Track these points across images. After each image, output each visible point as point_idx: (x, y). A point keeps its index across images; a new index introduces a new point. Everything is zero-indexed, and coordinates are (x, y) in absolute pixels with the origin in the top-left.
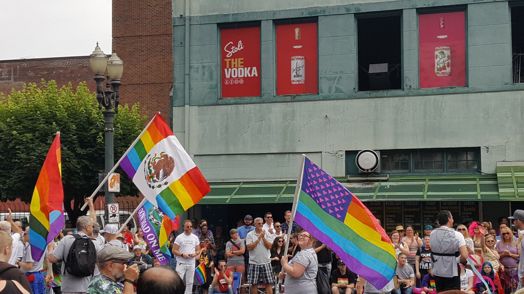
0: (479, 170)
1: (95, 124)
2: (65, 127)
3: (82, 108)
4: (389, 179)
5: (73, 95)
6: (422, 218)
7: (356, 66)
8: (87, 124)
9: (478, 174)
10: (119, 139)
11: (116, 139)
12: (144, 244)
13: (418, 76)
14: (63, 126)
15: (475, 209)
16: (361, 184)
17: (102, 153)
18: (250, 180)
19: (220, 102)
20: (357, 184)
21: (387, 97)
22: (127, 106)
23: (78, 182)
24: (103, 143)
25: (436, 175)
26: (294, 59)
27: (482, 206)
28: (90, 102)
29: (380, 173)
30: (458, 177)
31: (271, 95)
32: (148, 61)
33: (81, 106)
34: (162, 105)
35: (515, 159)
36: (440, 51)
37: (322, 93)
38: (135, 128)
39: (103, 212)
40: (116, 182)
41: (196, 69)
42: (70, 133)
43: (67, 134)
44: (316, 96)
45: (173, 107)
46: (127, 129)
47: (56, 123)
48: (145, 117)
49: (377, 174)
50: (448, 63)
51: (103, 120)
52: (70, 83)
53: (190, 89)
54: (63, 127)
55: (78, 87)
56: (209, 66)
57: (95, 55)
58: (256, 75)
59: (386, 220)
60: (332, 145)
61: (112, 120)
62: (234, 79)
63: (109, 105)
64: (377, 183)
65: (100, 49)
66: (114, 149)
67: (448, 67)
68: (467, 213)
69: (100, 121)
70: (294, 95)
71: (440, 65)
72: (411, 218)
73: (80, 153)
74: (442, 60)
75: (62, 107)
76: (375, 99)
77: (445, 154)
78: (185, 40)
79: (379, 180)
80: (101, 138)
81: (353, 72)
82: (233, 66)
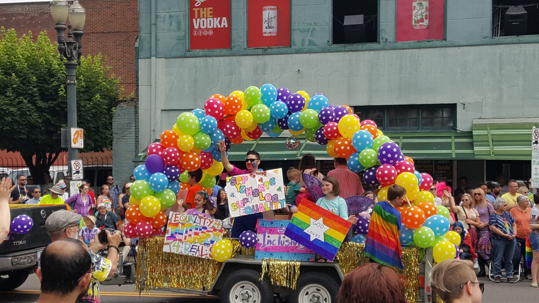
0: (454, 127)
1: (57, 76)
2: (25, 78)
5: (33, 44)
7: (330, 17)
8: (49, 76)
9: (453, 132)
10: (82, 92)
11: (79, 92)
14: (23, 78)
15: (449, 167)
17: (64, 106)
19: (188, 54)
22: (89, 57)
23: (40, 137)
24: (65, 96)
25: (410, 132)
26: (265, 9)
28: (51, 53)
31: (241, 48)
33: (42, 56)
34: (127, 55)
38: (99, 80)
39: (66, 168)
40: (79, 138)
41: (162, 19)
42: (30, 85)
43: (27, 86)
45: (139, 59)
46: (90, 82)
47: (15, 75)
51: (65, 72)
52: (30, 31)
53: (156, 41)
54: (23, 79)
55: (39, 36)
58: (226, 26)
61: (74, 72)
62: (203, 30)
66: (77, 103)
68: (442, 172)
71: (418, 17)
73: (41, 106)
74: (420, 12)
75: (21, 57)
76: (350, 53)
80: (63, 90)
81: (327, 24)
82: (201, 16)
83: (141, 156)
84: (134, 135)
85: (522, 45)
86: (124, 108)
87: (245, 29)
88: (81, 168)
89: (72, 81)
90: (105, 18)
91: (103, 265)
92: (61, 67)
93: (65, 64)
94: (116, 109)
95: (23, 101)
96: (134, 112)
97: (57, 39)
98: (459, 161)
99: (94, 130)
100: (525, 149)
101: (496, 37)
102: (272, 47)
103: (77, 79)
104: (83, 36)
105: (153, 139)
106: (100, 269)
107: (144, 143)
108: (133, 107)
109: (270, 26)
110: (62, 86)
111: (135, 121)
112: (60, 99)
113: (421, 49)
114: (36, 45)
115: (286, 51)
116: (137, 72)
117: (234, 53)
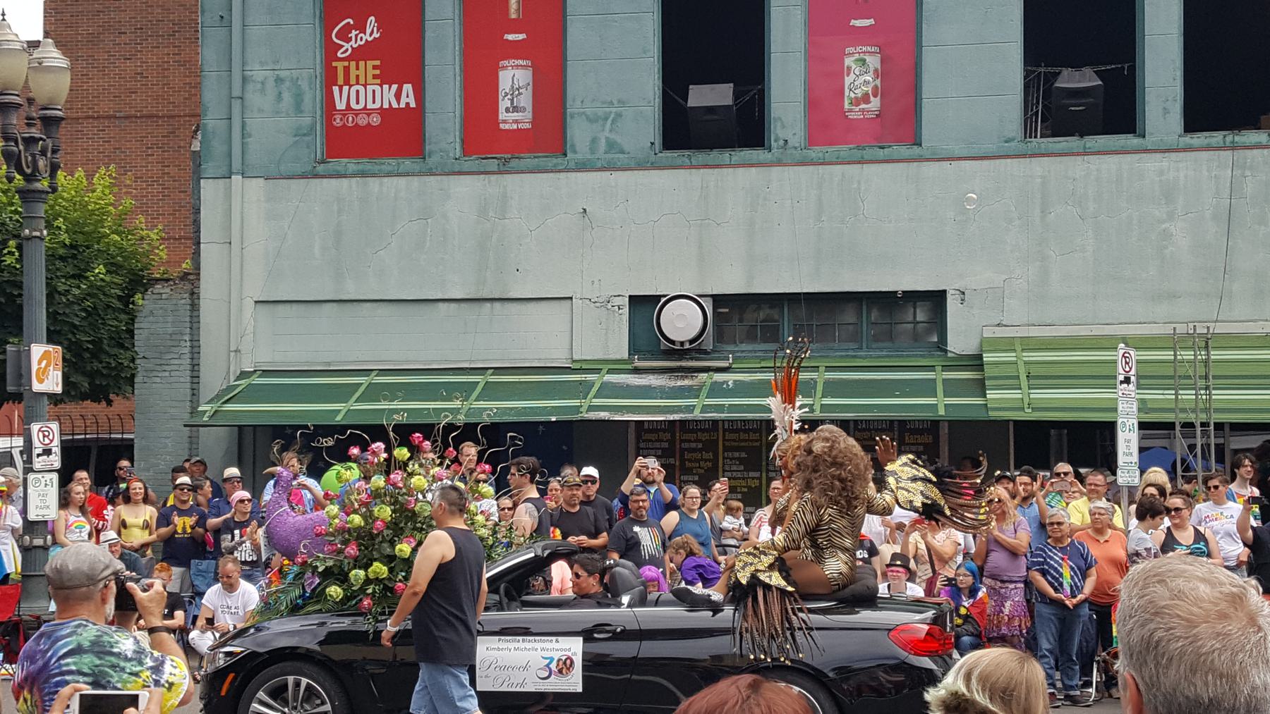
0: (941, 345)
7: (656, 88)
9: (940, 356)
11: (51, 257)
12: (84, 527)
13: (805, 116)
15: (931, 437)
16: (666, 376)
17: (16, 293)
19: (321, 169)
20: (656, 376)
22: (80, 173)
24: (18, 266)
26: (504, 68)
27: (946, 431)
30: (881, 362)
32: (138, 59)
34: (173, 171)
35: (1025, 320)
37: (575, 152)
39: (19, 442)
40: (51, 368)
41: (259, 86)
44: (559, 160)
45: (202, 181)
46: (80, 232)
48: (128, 202)
49: (705, 352)
50: (875, 88)
53: (243, 138)
56: (292, 78)
58: (413, 105)
59: (724, 464)
60: (596, 282)
61: (41, 210)
62: (357, 113)
63: (33, 171)
64: (703, 376)
66: (47, 284)
69: (12, 212)
77: (864, 307)
78: (231, 10)
79: (709, 367)
81: (649, 102)
82: (353, 81)
84: (188, 361)
86: (164, 296)
87: (458, 113)
88: (56, 442)
90: (117, 82)
91: (171, 674)
94: (143, 299)
96: (188, 307)
98: (952, 423)
99: (91, 346)
101: (1033, 139)
102: (522, 155)
103: (49, 225)
105: (235, 371)
106: (163, 686)
107: (213, 380)
109: (514, 107)
110: (11, 242)
111: (191, 328)
112: (5, 274)
115: (555, 166)
116: (198, 211)
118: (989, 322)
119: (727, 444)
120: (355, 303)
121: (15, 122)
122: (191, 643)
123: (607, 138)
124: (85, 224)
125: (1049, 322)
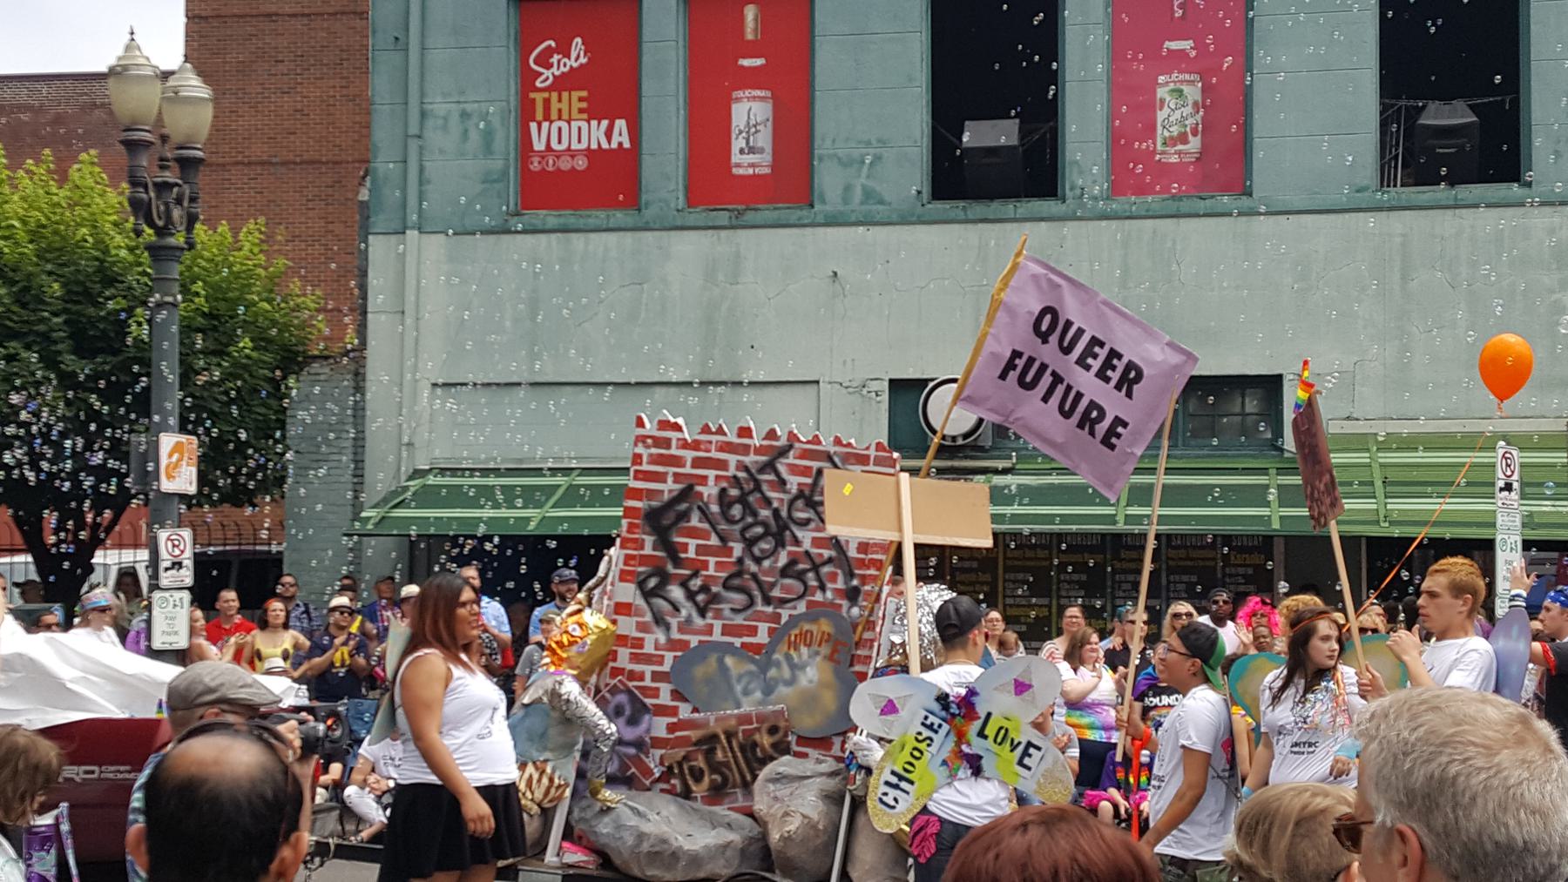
1: (123, 282)
2: (26, 289)
3: (84, 230)
4: (1018, 467)
6: (1109, 583)
8: (100, 282)
11: (187, 329)
14: (20, 285)
18: (602, 462)
21: (1015, 220)
22: (223, 228)
26: (738, 100)
28: (109, 215)
29: (992, 448)
31: (668, 206)
33: (79, 225)
36: (1172, 86)
37: (824, 202)
38: (249, 297)
39: (143, 555)
41: (440, 122)
44: (805, 212)
45: (370, 237)
48: (281, 262)
49: (982, 449)
51: (149, 270)
52: (47, 151)
53: (421, 183)
54: (20, 291)
55: (76, 166)
57: (125, 68)
58: (627, 145)
59: (1004, 588)
60: (849, 362)
61: (176, 271)
65: (139, 49)
66: (182, 362)
67: (1195, 133)
68: (1241, 570)
69: (139, 274)
70: (739, 207)
72: (1078, 582)
74: (1177, 115)
76: (980, 225)
78: (407, 30)
82: (554, 115)
83: (369, 518)
84: (351, 457)
85: (1464, 211)
86: (322, 377)
89: (167, 295)
92: (136, 255)
93: (150, 248)
95: (17, 354)
97: (125, 174)
98: (1288, 539)
100: (1480, 506)
101: (1391, 189)
102: (760, 206)
103: (185, 290)
104: (202, 168)
105: (405, 470)
107: (379, 481)
108: (349, 377)
113: (1182, 221)
114: (63, 193)
115: (799, 219)
116: (363, 274)
117: (647, 223)
118: (1337, 415)
119: (1009, 563)
120: (554, 387)
121: (145, 164)
122: (347, 801)
123: (864, 187)
124: (229, 289)
125: (1410, 415)
